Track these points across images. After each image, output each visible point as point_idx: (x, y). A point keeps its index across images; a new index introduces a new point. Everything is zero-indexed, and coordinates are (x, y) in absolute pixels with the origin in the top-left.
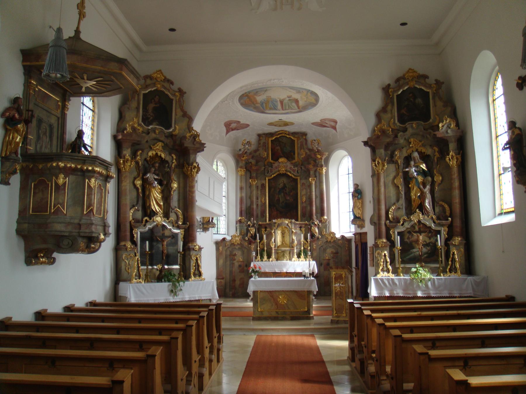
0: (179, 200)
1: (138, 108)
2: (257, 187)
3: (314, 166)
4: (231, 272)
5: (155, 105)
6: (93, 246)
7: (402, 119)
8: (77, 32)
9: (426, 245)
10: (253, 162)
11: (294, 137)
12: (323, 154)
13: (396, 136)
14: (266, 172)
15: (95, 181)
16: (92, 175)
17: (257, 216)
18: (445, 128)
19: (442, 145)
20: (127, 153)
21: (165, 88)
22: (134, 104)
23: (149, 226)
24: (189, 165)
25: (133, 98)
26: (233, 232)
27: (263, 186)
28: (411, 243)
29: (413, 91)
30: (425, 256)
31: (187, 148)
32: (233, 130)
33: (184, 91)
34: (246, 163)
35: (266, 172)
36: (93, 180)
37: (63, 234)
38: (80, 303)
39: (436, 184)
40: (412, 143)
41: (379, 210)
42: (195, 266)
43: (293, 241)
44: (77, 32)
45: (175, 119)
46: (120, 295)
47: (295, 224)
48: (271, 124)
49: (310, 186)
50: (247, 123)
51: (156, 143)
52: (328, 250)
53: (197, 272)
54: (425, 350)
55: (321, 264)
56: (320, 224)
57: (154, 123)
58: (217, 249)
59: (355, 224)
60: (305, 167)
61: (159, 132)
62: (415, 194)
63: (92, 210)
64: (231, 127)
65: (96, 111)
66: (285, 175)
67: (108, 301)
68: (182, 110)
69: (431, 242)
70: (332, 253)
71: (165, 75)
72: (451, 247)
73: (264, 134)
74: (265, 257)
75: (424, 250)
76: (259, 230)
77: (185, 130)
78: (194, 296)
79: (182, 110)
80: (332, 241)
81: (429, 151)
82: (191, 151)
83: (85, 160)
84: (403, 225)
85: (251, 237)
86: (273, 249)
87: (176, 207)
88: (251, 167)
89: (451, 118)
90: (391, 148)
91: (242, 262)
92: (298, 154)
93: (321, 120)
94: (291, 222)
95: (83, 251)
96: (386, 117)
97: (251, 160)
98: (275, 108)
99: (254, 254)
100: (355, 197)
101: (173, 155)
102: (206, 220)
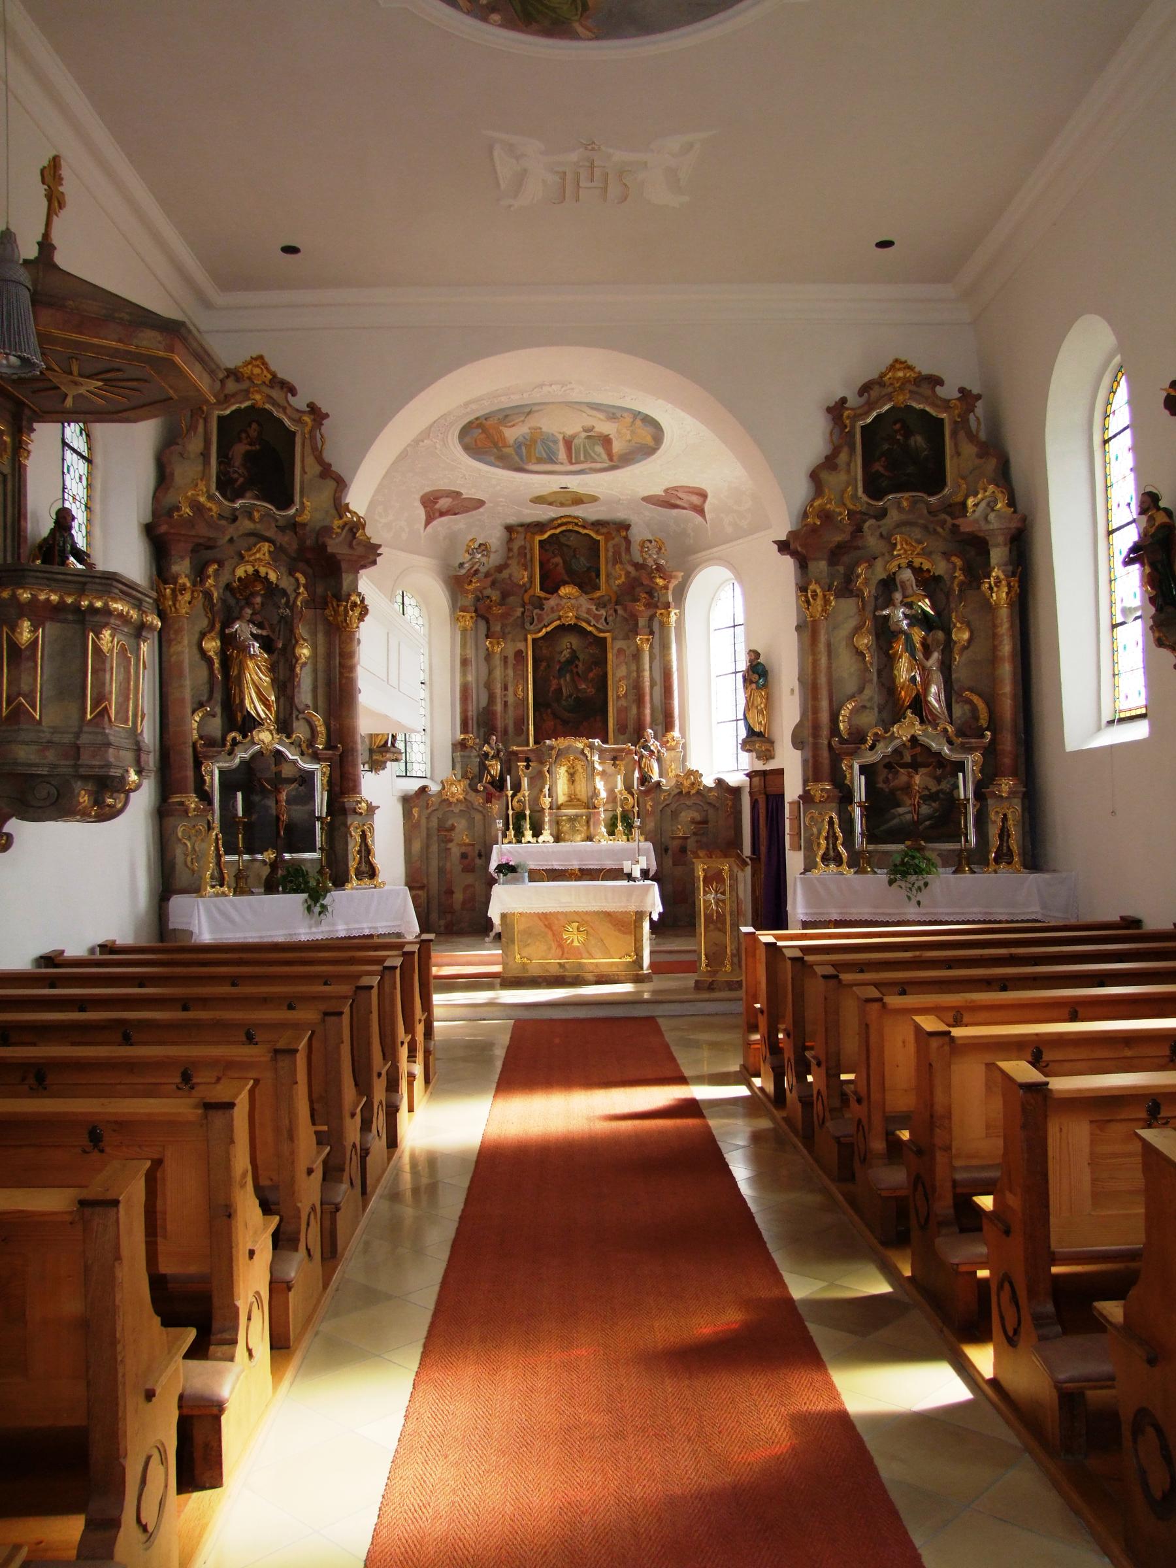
0: (315, 689)
1: (205, 455)
2: (505, 659)
3: (648, 605)
4: (441, 871)
5: (248, 447)
6: (110, 801)
7: (874, 488)
8: (46, 246)
9: (929, 797)
10: (495, 595)
11: (597, 532)
12: (671, 577)
13: (859, 530)
14: (527, 620)
15: (112, 636)
16: (104, 620)
17: (505, 732)
18: (983, 509)
19: (973, 549)
20: (182, 568)
21: (274, 403)
22: (195, 445)
23: (242, 755)
24: (339, 600)
25: (192, 427)
26: (445, 770)
27: (520, 655)
28: (892, 792)
29: (901, 415)
30: (927, 823)
31: (333, 556)
32: (442, 514)
33: (324, 410)
34: (478, 599)
35: (527, 620)
36: (106, 634)
37: (34, 771)
38: (76, 949)
39: (956, 649)
40: (899, 547)
41: (816, 711)
42: (359, 852)
43: (595, 793)
44: (46, 246)
45: (302, 482)
46: (171, 927)
47: (602, 752)
48: (539, 500)
49: (637, 656)
50: (479, 496)
51: (255, 545)
52: (683, 814)
53: (364, 868)
54: (943, 1027)
55: (666, 850)
56: (663, 750)
57: (248, 494)
58: (407, 814)
59: (749, 751)
60: (625, 609)
61: (262, 517)
62: (904, 671)
63: (106, 710)
64: (437, 506)
65: (98, 459)
66: (575, 629)
67: (143, 943)
69: (941, 791)
70: (693, 821)
71: (273, 368)
72: (990, 802)
73: (522, 525)
74: (528, 834)
75: (925, 810)
76: (508, 768)
77: (327, 512)
78: (357, 926)
79: (320, 459)
80: (693, 792)
81: (940, 567)
82: (344, 566)
83: (85, 584)
84: (872, 748)
85: (492, 783)
86: (547, 811)
87: (307, 707)
88: (490, 608)
89: (997, 485)
90: (846, 559)
91: (468, 845)
92: (608, 576)
93: (666, 491)
94: (591, 747)
95: (84, 816)
96: (835, 480)
97: (488, 592)
98: (551, 460)
99: (500, 824)
100: (751, 682)
101: (298, 575)
102: (379, 742)
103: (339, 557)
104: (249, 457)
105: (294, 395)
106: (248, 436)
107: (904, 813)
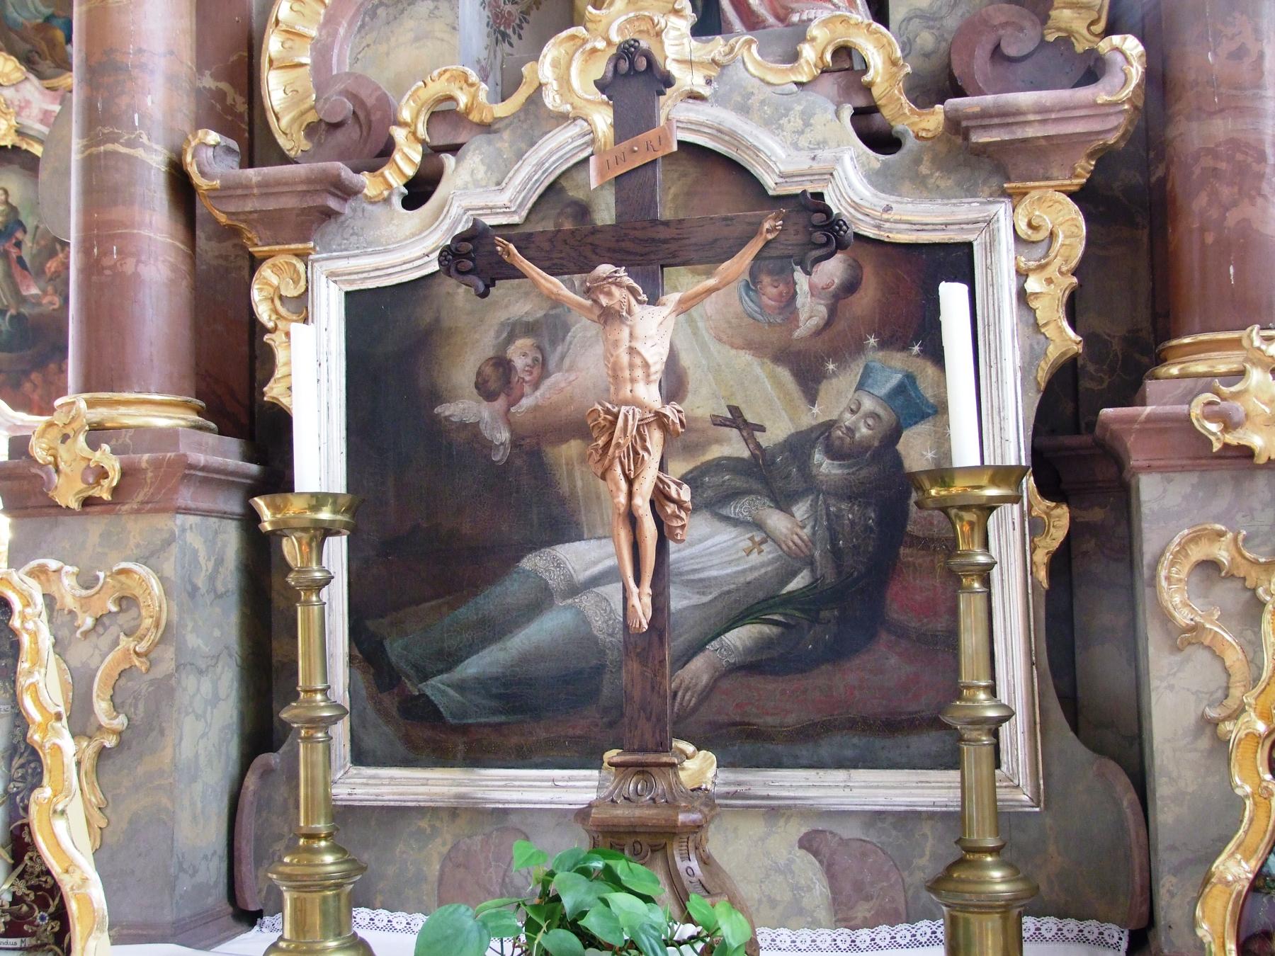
28: (532, 445)
30: (740, 637)
69: (824, 435)
72: (1158, 495)
75: (717, 550)
84: (419, 191)
107: (587, 583)
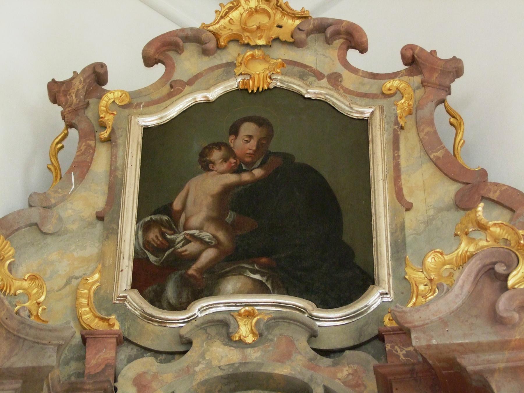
1: (107, 218)
5: (232, 178)
33: (444, 54)
57: (231, 284)
68: (449, 166)
71: (296, 7)
79: (449, 166)
103: (471, 363)
104: (230, 201)
105: (363, 50)
106: (230, 152)
